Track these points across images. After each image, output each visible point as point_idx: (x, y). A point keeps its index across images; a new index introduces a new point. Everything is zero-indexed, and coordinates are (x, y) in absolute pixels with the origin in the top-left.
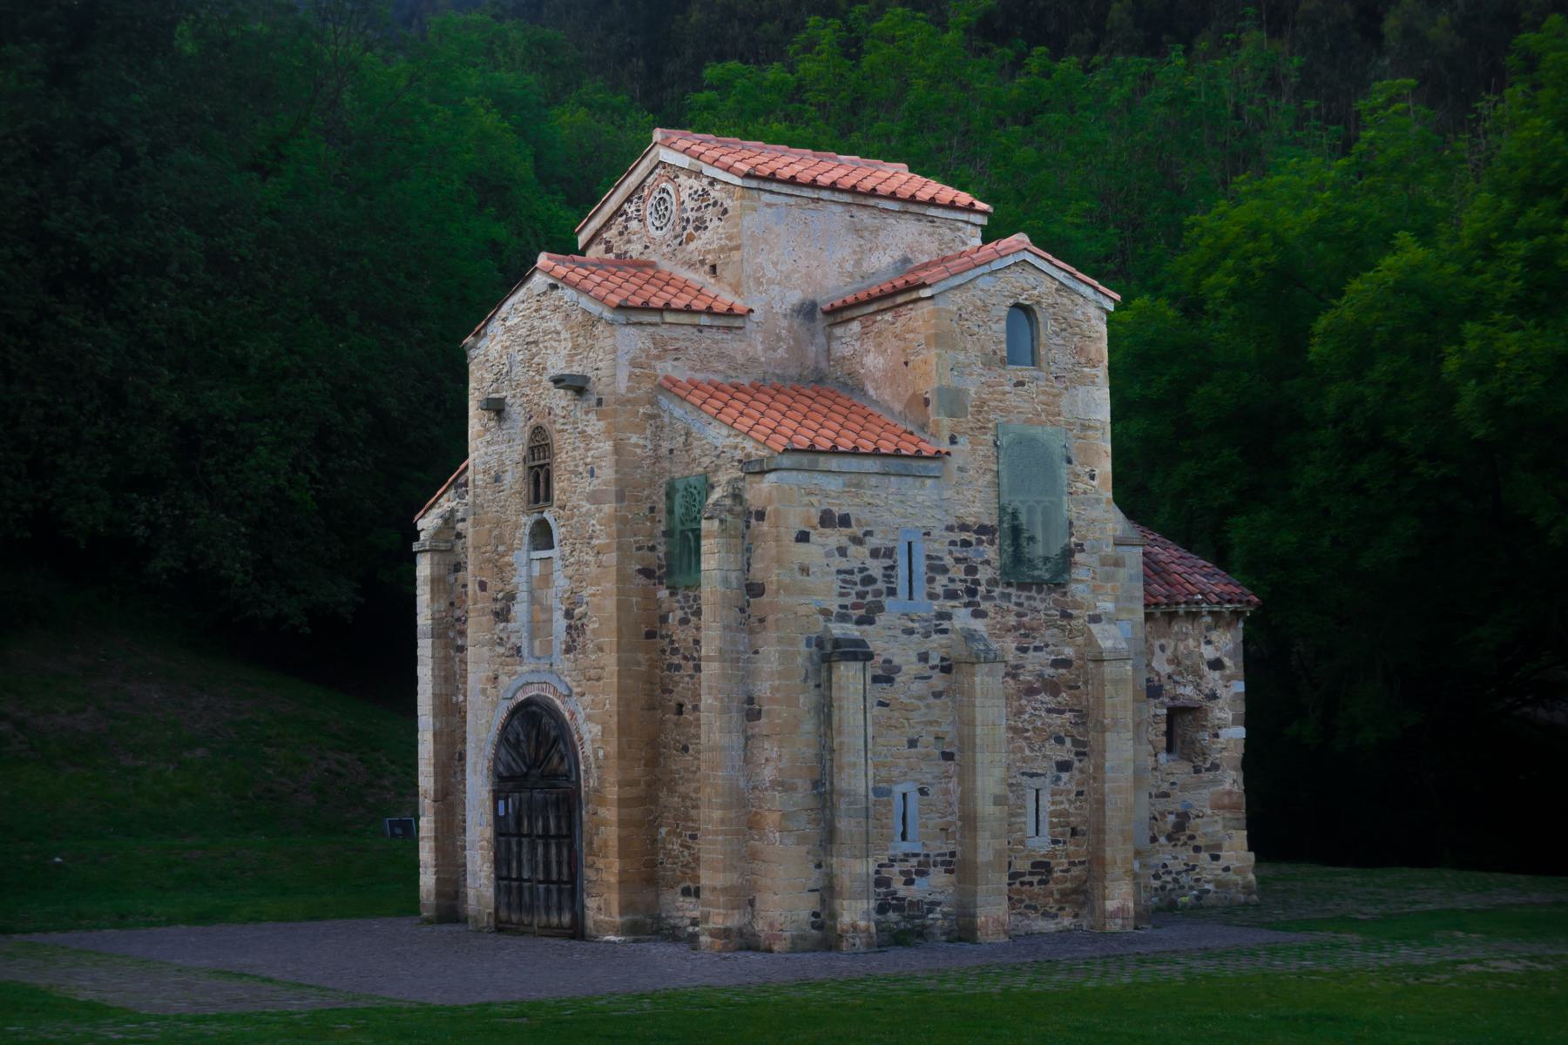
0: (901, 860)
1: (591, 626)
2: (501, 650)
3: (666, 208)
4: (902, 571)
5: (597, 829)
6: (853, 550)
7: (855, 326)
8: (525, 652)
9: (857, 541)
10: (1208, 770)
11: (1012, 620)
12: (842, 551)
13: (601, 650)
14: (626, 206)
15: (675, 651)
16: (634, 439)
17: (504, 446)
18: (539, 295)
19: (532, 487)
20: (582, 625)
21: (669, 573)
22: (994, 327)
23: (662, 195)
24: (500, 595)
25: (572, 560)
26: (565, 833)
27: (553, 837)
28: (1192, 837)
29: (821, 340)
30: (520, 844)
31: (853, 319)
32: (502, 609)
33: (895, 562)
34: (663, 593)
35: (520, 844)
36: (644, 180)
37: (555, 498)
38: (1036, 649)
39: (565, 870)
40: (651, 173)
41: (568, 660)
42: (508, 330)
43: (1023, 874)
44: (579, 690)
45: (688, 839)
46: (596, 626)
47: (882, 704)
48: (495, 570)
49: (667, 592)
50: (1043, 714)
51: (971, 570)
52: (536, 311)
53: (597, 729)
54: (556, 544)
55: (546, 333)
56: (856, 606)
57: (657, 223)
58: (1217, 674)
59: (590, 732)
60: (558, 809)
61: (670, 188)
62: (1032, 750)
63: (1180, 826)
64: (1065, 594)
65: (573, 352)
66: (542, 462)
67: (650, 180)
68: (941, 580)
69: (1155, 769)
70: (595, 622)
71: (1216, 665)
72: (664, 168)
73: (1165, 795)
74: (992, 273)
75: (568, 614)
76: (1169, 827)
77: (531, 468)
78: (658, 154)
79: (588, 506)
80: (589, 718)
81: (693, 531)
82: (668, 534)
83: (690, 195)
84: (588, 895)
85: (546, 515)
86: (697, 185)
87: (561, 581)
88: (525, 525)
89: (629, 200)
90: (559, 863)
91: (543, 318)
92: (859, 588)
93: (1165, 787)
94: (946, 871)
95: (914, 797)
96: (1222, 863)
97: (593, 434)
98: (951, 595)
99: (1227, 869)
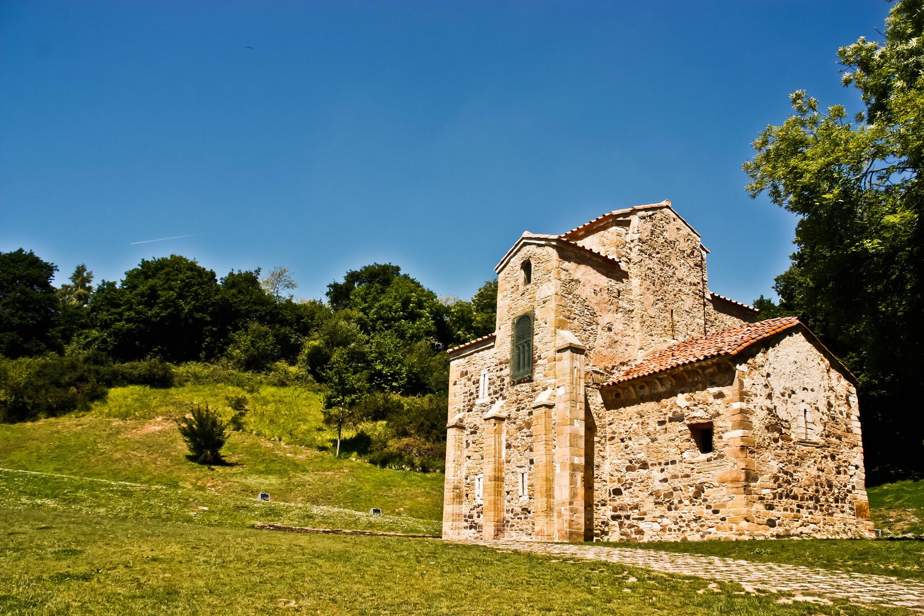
6: (468, 383)
9: (469, 380)
10: (715, 459)
11: (514, 398)
28: (705, 500)
38: (523, 409)
43: (518, 514)
47: (473, 443)
50: (525, 438)
51: (503, 380)
56: (468, 405)
58: (719, 401)
63: (697, 495)
68: (493, 387)
69: (681, 461)
73: (687, 476)
76: (691, 494)
92: (469, 398)
93: (688, 471)
96: (720, 515)
98: (495, 393)
99: (723, 519)
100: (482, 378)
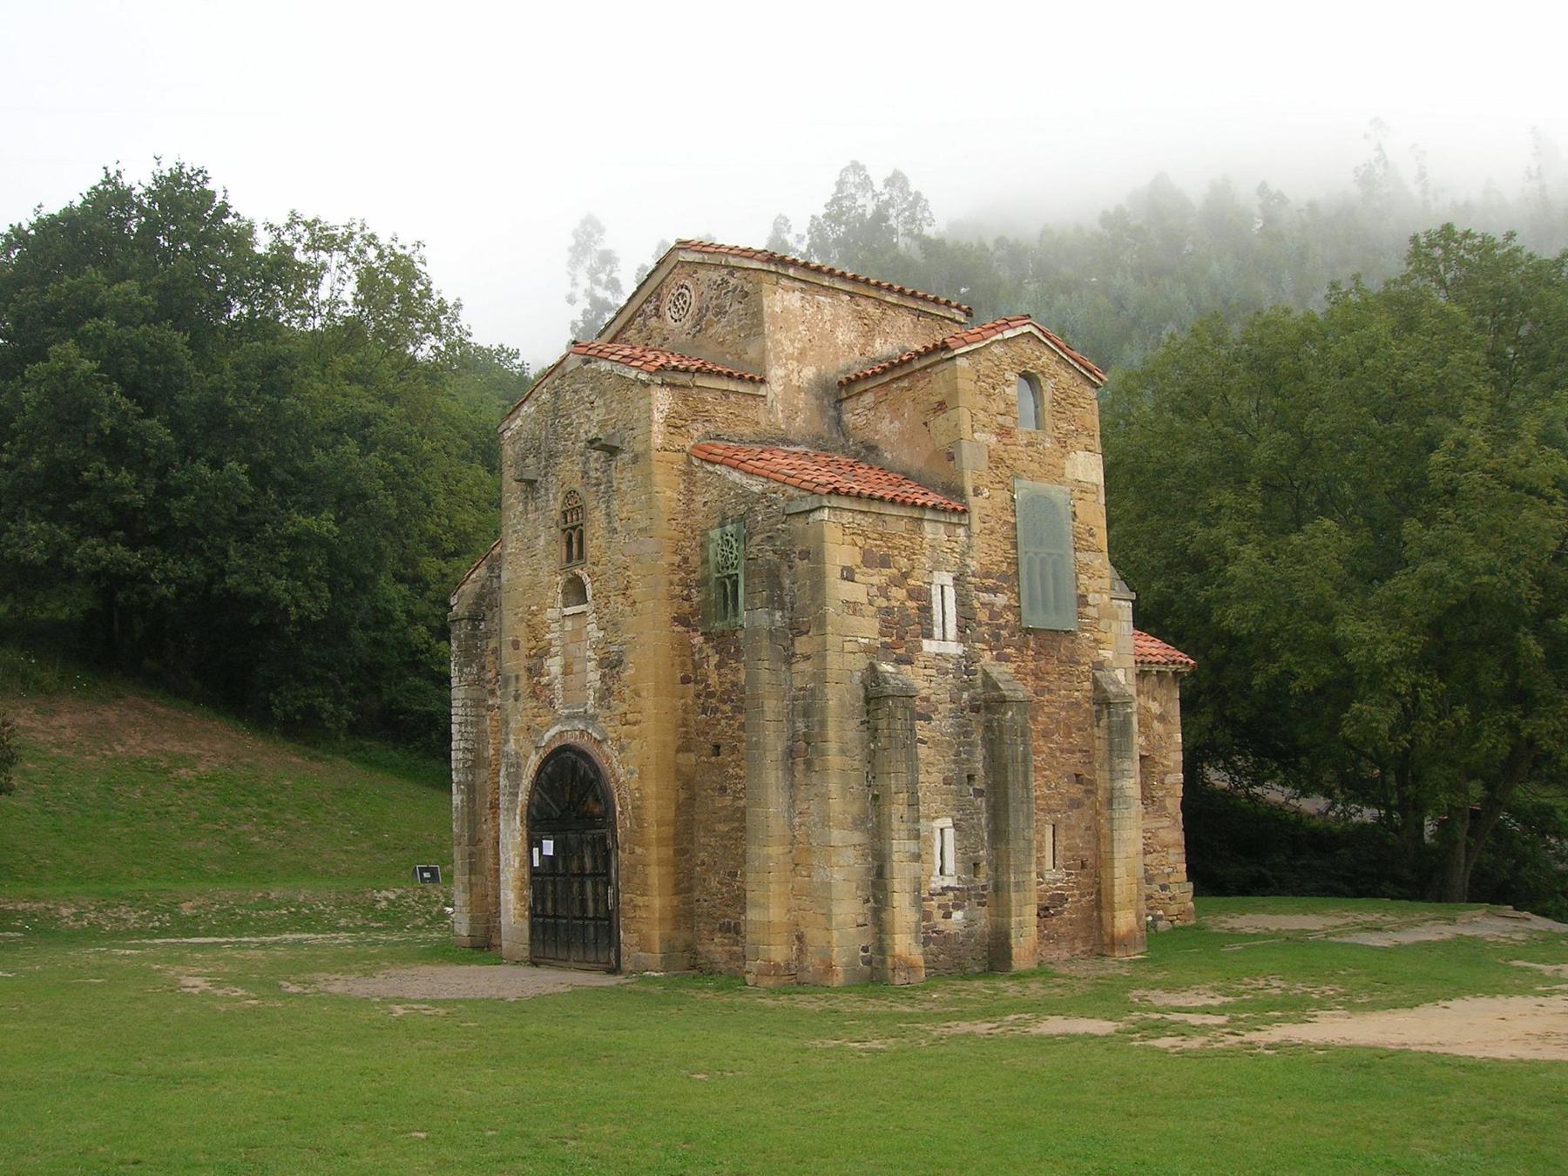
0: (940, 894)
3: (685, 302)
4: (937, 617)
7: (868, 398)
12: (883, 592)
14: (644, 306)
15: (711, 695)
16: (669, 493)
19: (564, 548)
21: (704, 622)
22: (1008, 390)
23: (680, 291)
29: (832, 413)
31: (866, 391)
33: (931, 602)
34: (698, 640)
35: (554, 884)
36: (663, 281)
37: (589, 555)
39: (601, 908)
40: (670, 273)
49: (702, 638)
54: (589, 598)
60: (594, 847)
61: (687, 283)
62: (1049, 788)
64: (1073, 641)
65: (607, 417)
66: (575, 523)
67: (667, 280)
70: (631, 668)
71: (1162, 718)
74: (1006, 341)
75: (602, 663)
77: (564, 530)
81: (729, 577)
82: (703, 582)
83: (709, 286)
84: (627, 931)
85: (578, 571)
86: (716, 276)
89: (647, 301)
94: (979, 904)
95: (950, 834)
100: (936, 591)
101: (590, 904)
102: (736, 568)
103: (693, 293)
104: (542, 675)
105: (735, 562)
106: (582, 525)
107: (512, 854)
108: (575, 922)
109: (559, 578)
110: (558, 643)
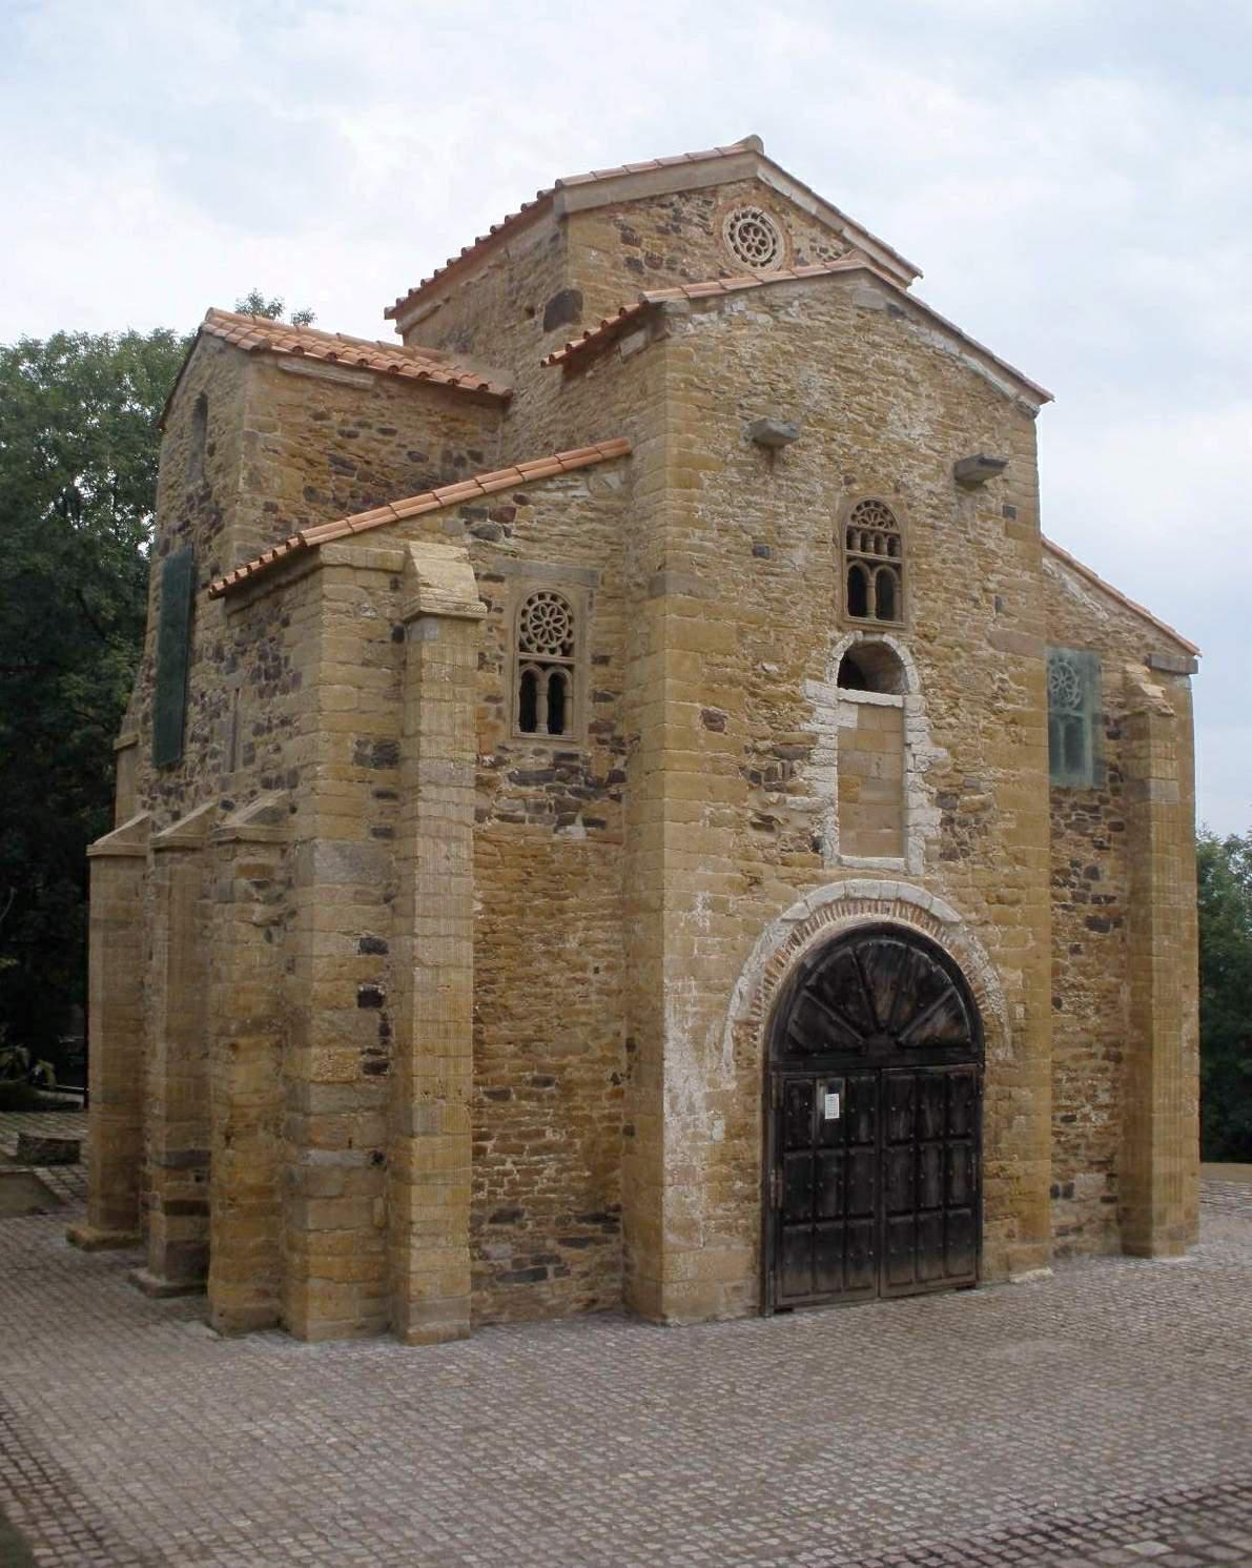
1: (1001, 825)
2: (769, 838)
5: (1010, 1120)
8: (832, 846)
13: (1023, 863)
17: (782, 504)
18: (861, 308)
20: (977, 822)
23: (749, 220)
24: (762, 745)
25: (953, 720)
26: (960, 1131)
27: (929, 1140)
30: (847, 1162)
32: (771, 772)
37: (914, 620)
41: (950, 870)
42: (794, 328)
44: (973, 916)
45: (1058, 1123)
46: (1012, 826)
48: (750, 700)
52: (858, 329)
53: (1016, 976)
55: (881, 367)
57: (749, 256)
59: (1002, 980)
61: (766, 216)
65: (947, 421)
66: (871, 555)
67: (728, 189)
70: (1010, 820)
72: (757, 188)
75: (941, 799)
77: (850, 559)
78: (755, 169)
79: (991, 650)
80: (993, 960)
85: (888, 639)
86: (823, 242)
87: (922, 746)
88: (834, 643)
90: (946, 1182)
91: (874, 345)
97: (1001, 553)
101: (933, 1186)
102: (1079, 708)
103: (781, 241)
104: (791, 791)
105: (1077, 701)
106: (898, 567)
107: (704, 1116)
108: (898, 1220)
109: (837, 634)
110: (834, 743)
